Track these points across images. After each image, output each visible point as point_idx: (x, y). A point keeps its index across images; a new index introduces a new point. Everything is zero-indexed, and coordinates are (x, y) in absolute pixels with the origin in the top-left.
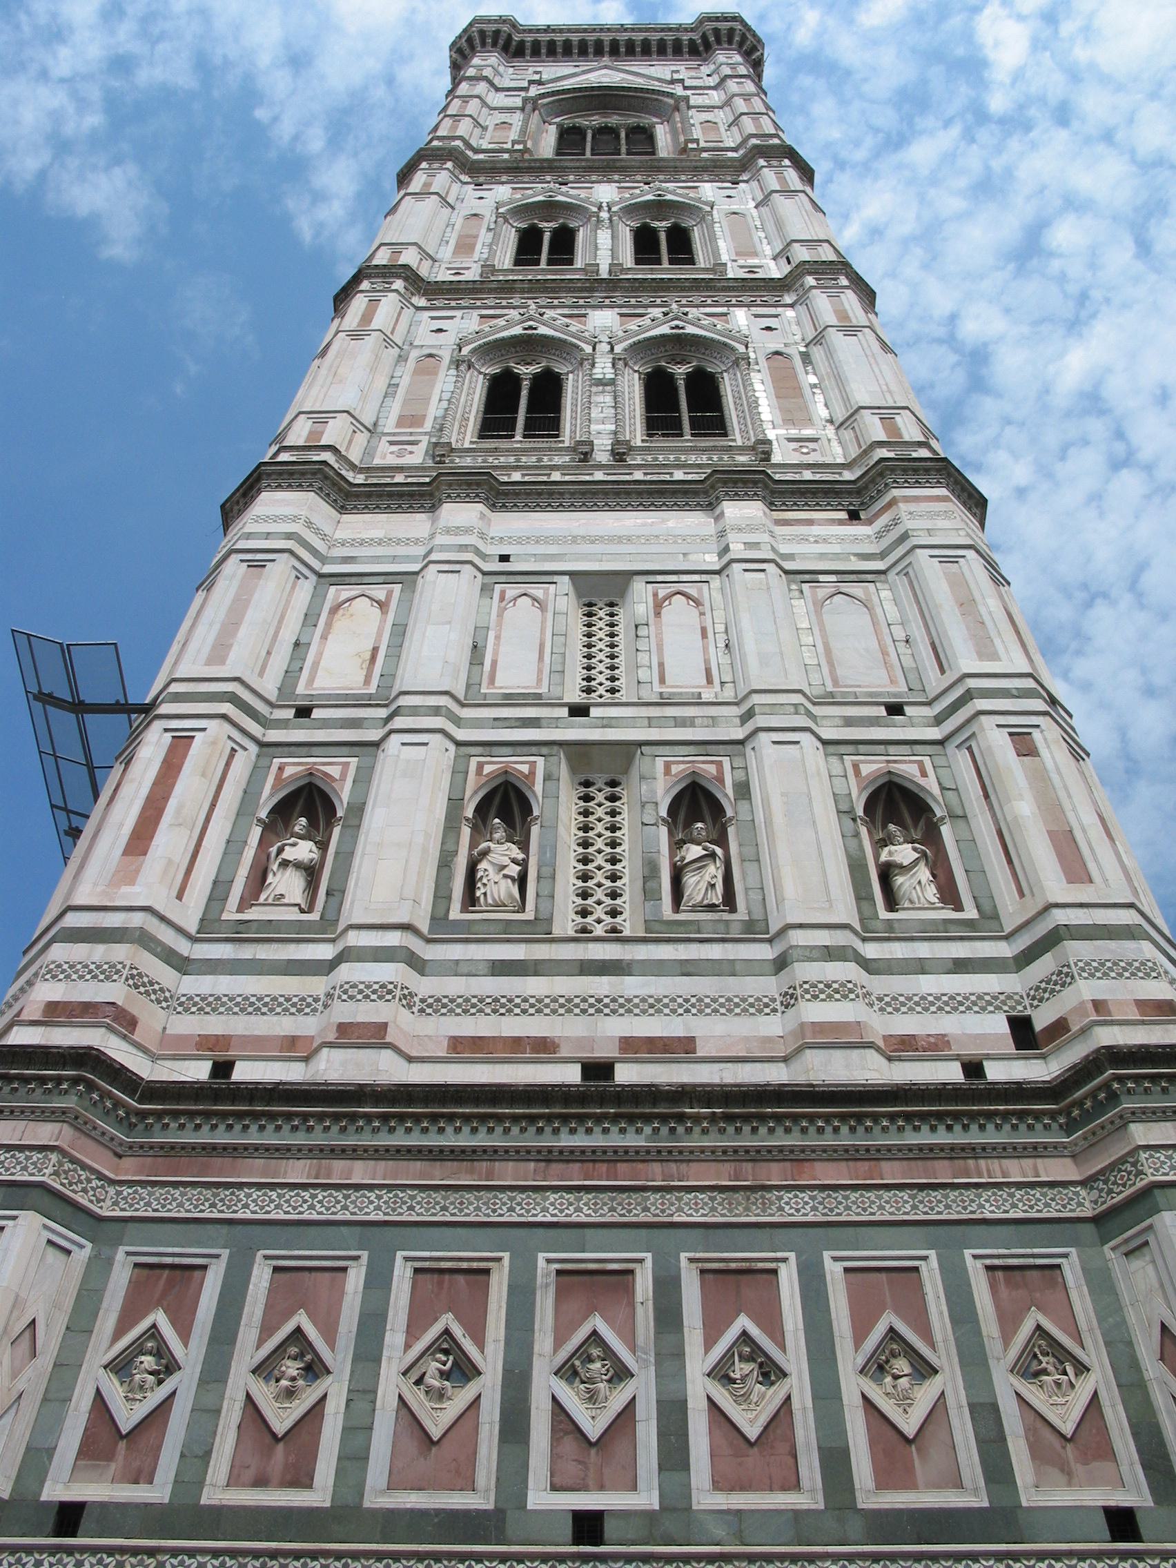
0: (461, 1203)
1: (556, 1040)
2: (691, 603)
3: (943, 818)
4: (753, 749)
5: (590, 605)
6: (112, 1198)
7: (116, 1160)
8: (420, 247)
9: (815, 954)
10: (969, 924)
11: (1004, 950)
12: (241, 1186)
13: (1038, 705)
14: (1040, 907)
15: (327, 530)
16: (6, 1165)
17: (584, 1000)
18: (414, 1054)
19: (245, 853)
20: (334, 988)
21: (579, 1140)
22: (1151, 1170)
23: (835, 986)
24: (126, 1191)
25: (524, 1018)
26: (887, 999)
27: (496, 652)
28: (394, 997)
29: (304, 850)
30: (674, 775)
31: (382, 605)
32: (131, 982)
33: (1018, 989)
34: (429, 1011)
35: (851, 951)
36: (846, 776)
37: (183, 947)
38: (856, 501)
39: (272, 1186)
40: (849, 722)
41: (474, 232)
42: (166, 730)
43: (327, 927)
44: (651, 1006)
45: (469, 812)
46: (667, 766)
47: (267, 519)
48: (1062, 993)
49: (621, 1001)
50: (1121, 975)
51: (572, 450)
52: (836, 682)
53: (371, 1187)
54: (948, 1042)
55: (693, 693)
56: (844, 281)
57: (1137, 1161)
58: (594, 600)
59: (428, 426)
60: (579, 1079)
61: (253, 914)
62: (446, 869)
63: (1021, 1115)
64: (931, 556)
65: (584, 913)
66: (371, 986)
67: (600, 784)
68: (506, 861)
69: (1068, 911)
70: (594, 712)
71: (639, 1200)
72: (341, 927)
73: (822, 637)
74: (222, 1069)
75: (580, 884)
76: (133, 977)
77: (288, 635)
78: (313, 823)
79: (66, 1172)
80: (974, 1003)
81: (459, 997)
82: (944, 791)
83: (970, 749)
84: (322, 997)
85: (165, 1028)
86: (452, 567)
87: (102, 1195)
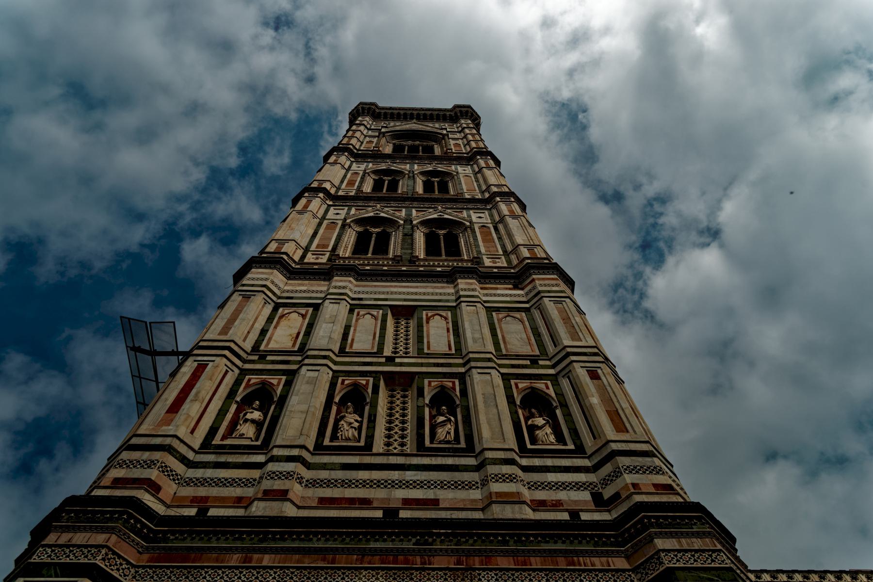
0: (318, 576)
1: (371, 500)
2: (443, 318)
3: (556, 407)
4: (469, 376)
7: (138, 555)
8: (331, 182)
11: (586, 463)
12: (202, 568)
13: (601, 359)
14: (604, 442)
15: (281, 285)
17: (386, 481)
18: (301, 505)
19: (227, 416)
21: (378, 545)
22: (667, 562)
24: (141, 571)
25: (357, 490)
28: (293, 478)
29: (256, 415)
30: (433, 387)
31: (304, 316)
33: (595, 480)
34: (310, 485)
37: (191, 455)
38: (517, 281)
39: (220, 568)
41: (355, 179)
42: (195, 361)
45: (337, 399)
46: (430, 383)
47: (253, 279)
49: (404, 482)
50: (645, 472)
51: (392, 259)
52: (507, 350)
53: (271, 568)
54: (562, 503)
56: (513, 200)
57: (660, 557)
59: (330, 248)
63: (600, 537)
64: (550, 301)
68: (352, 421)
69: (618, 444)
71: (408, 574)
74: (203, 511)
75: (386, 440)
77: (259, 326)
79: (109, 559)
80: (574, 486)
84: (258, 479)
86: (337, 301)
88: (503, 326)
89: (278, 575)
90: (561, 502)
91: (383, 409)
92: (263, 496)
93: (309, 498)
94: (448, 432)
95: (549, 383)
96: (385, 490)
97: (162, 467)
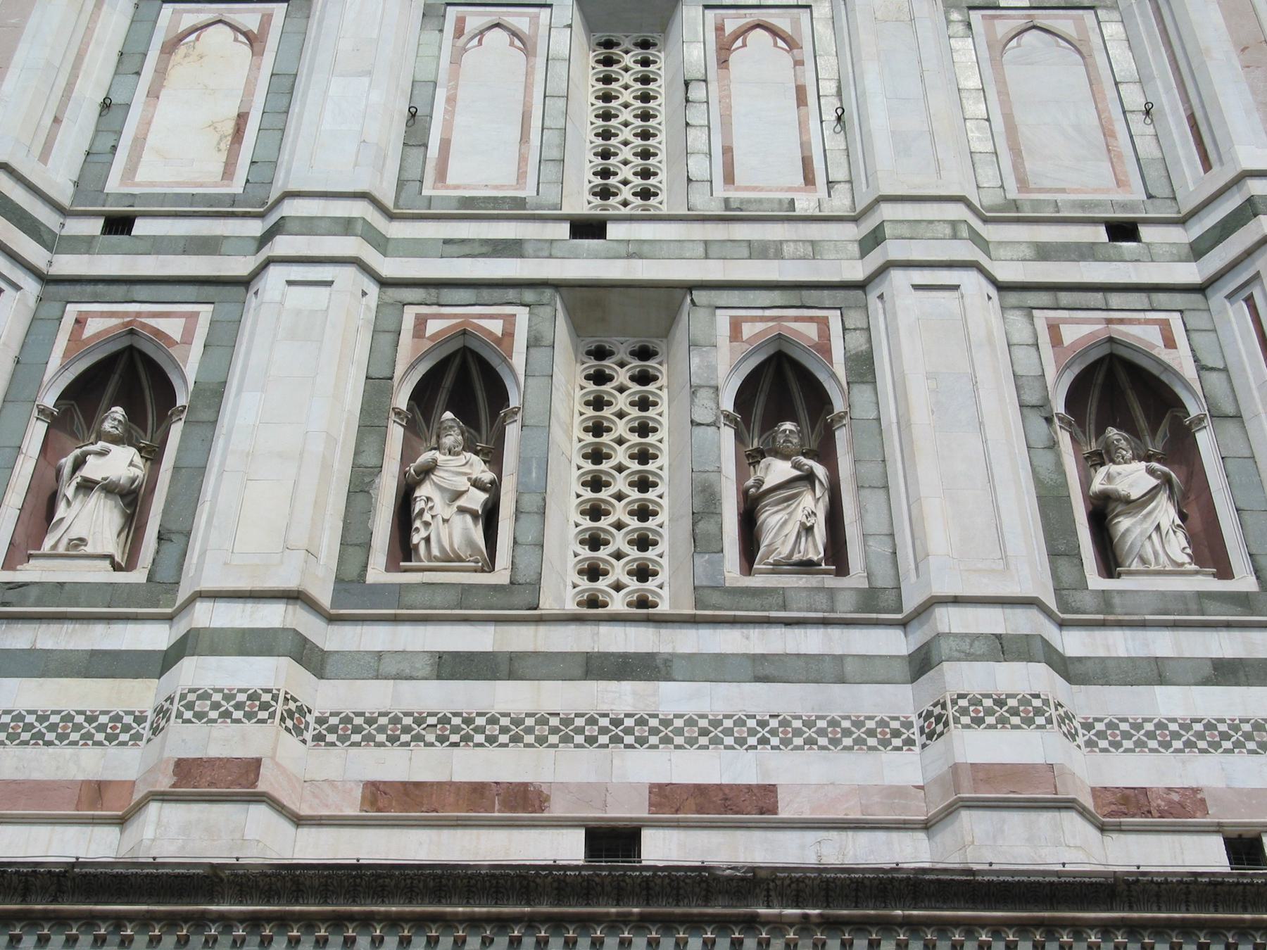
1: (545, 789)
2: (780, 43)
3: (1200, 420)
4: (881, 297)
5: (609, 44)
9: (980, 648)
10: (1241, 600)
17: (592, 721)
18: (305, 811)
20: (170, 699)
23: (1012, 703)
25: (491, 752)
26: (1100, 726)
27: (448, 125)
28: (272, 716)
30: (748, 341)
31: (254, 40)
34: (331, 738)
35: (1039, 644)
36: (1036, 346)
40: (1044, 252)
44: (704, 732)
45: (402, 400)
46: (736, 326)
49: (654, 723)
52: (1023, 184)
54: (1203, 801)
55: (780, 201)
58: (615, 36)
60: (582, 856)
61: (31, 572)
62: (360, 497)
65: (593, 572)
66: (233, 697)
67: (622, 354)
68: (463, 483)
70: (613, 230)
72: (183, 595)
73: (1002, 103)
77: (90, 92)
78: (135, 416)
80: (1249, 737)
81: (381, 714)
82: (1203, 373)
83: (1250, 301)
84: (150, 715)
88: (1010, 71)
91: (568, 433)
92: (174, 786)
93: (331, 783)
94: (802, 524)
95: (1175, 320)
96: (591, 752)
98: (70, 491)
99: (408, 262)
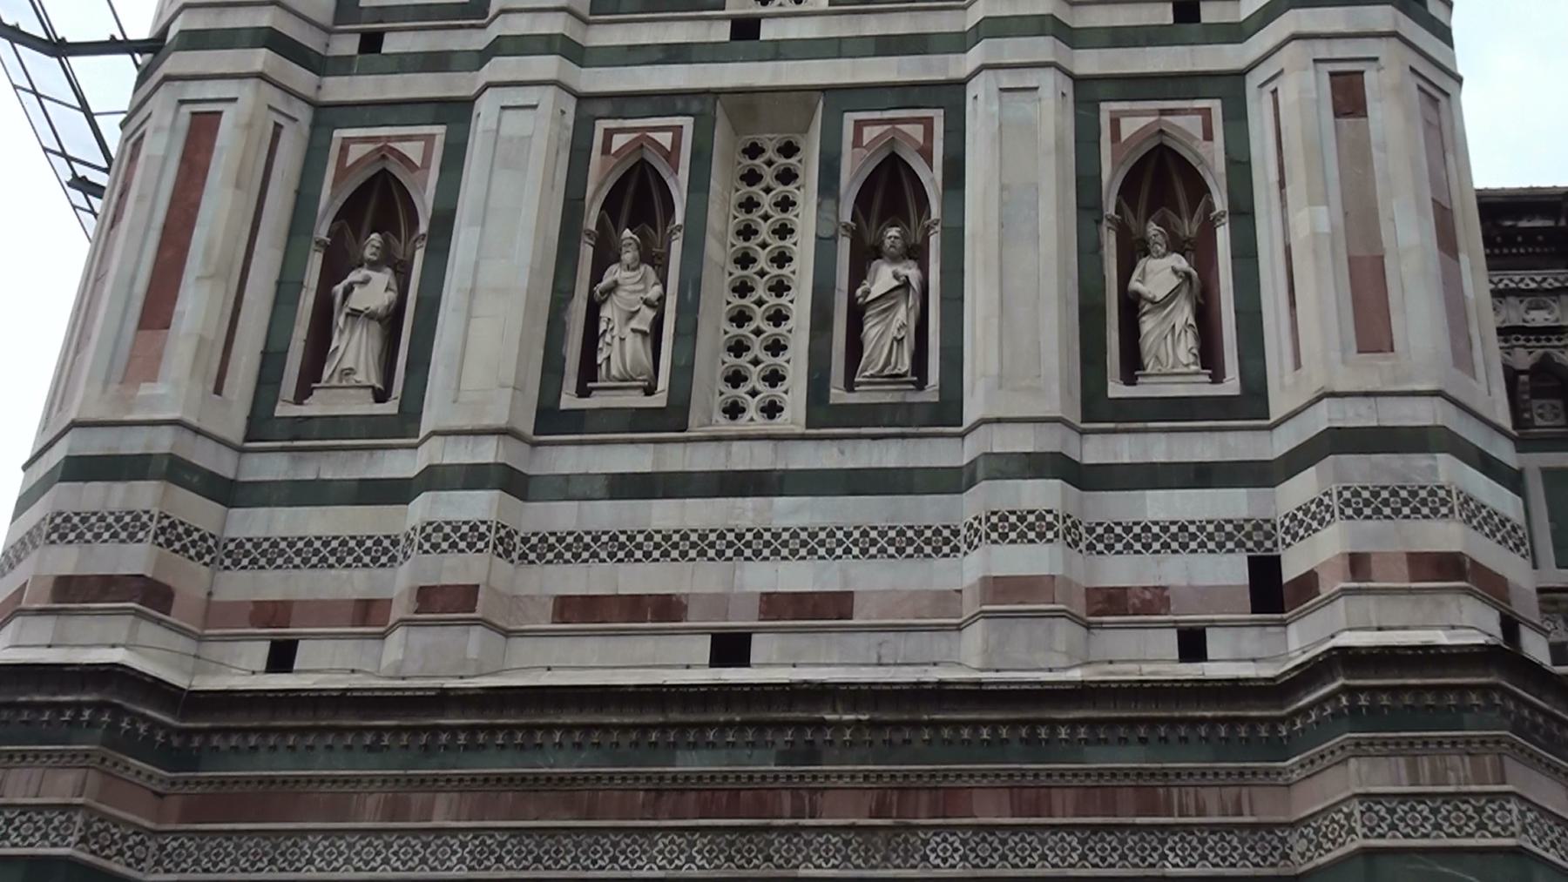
0: (557, 852)
1: (683, 600)
6: (154, 856)
12: (304, 833)
16: (22, 831)
28: (487, 545)
32: (161, 539)
43: (405, 425)
46: (859, 126)
48: (1318, 534)
54: (1168, 599)
61: (312, 407)
72: (422, 434)
76: (163, 530)
79: (95, 835)
83: (1275, 92)
85: (210, 594)
87: (142, 853)
89: (470, 852)
90: (1166, 593)
93: (532, 598)
97: (163, 530)
98: (340, 320)
99: (599, 72)
